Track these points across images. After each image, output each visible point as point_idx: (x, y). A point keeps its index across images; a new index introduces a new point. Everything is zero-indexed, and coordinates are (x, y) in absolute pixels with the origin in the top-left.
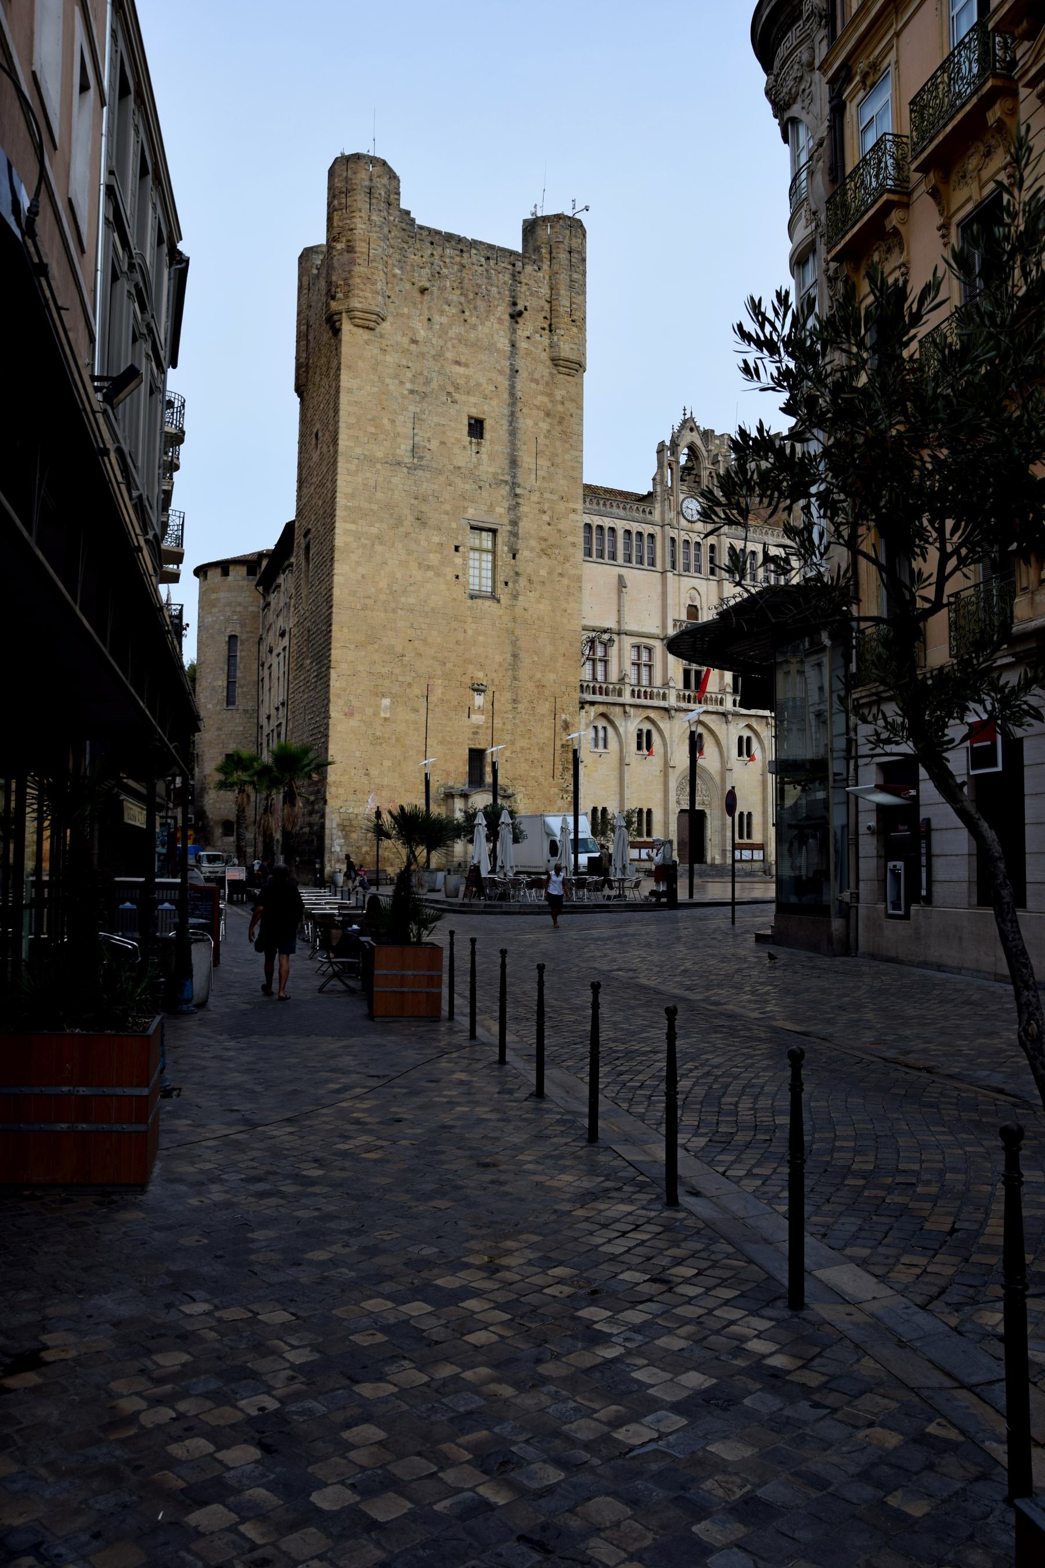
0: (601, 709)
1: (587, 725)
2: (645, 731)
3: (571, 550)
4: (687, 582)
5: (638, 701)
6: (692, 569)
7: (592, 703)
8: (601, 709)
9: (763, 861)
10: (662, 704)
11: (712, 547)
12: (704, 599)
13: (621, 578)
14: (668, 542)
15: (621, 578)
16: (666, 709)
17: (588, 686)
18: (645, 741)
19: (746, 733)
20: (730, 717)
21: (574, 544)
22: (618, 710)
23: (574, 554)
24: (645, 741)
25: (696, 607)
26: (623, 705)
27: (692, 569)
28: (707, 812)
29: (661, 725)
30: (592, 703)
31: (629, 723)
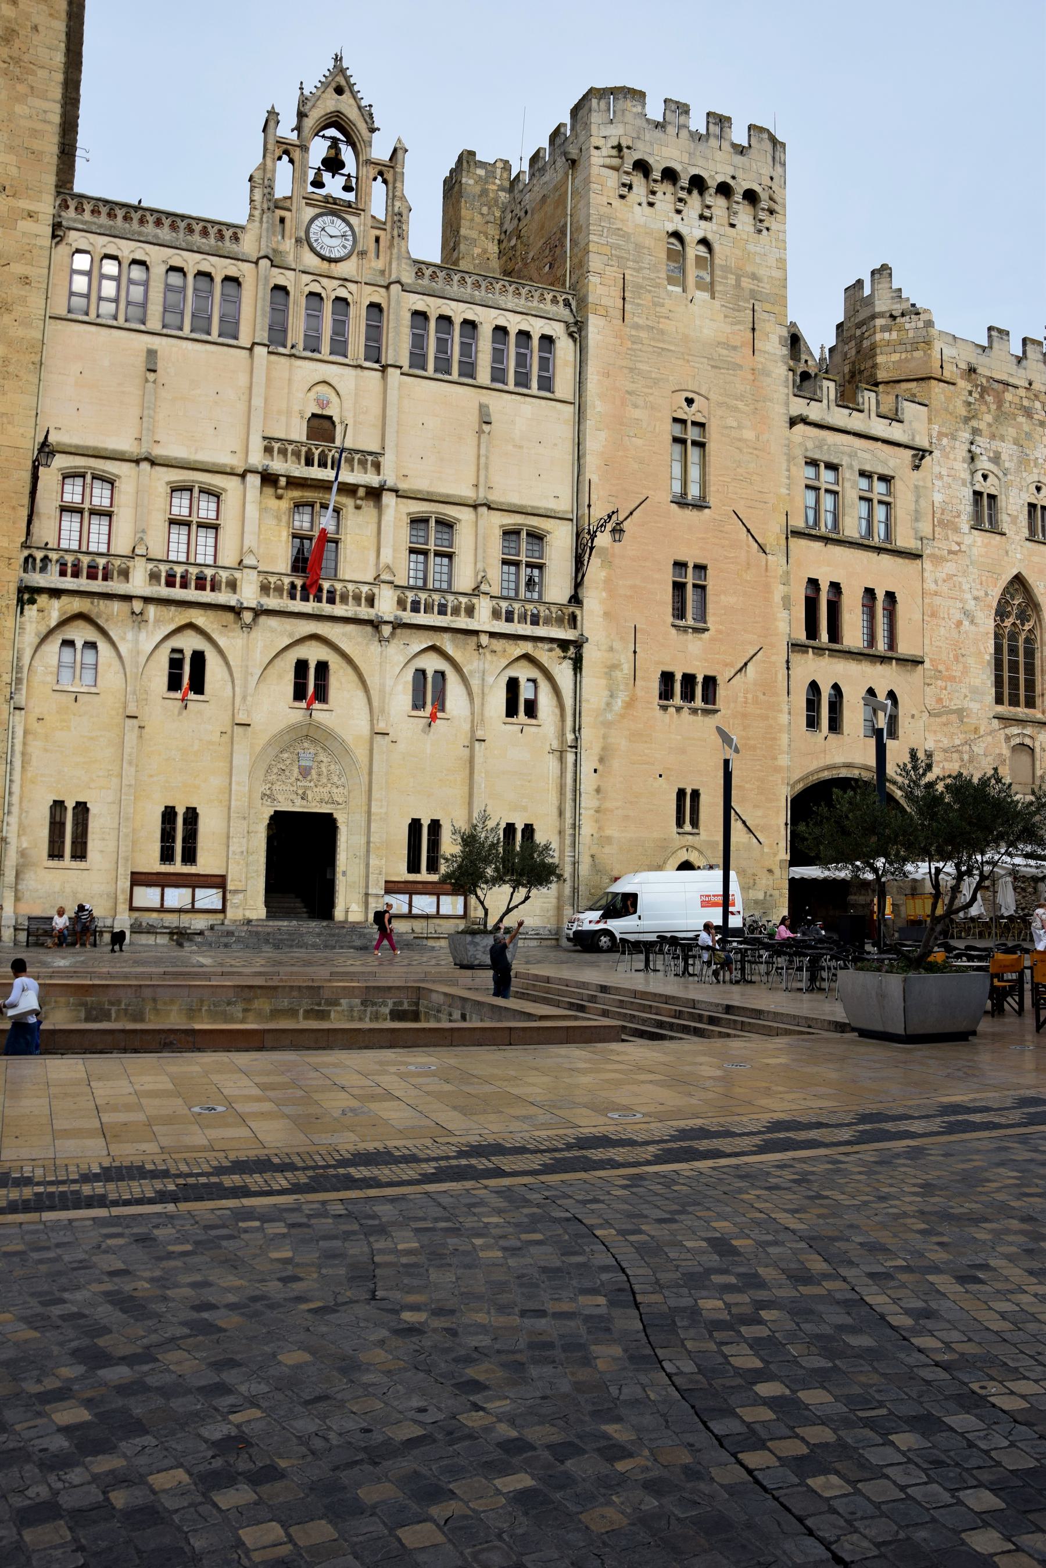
0: (77, 605)
1: (43, 640)
2: (188, 655)
3: (16, 290)
4: (309, 371)
5: (164, 592)
6: (326, 347)
7: (56, 593)
8: (77, 605)
9: (465, 916)
10: (223, 597)
11: (375, 307)
12: (348, 404)
13: (152, 354)
14: (265, 294)
15: (152, 354)
16: (230, 609)
17: (46, 559)
18: (188, 675)
19: (432, 664)
20: (387, 630)
21: (25, 280)
22: (116, 606)
23: (23, 300)
24: (188, 675)
25: (330, 418)
26: (127, 598)
27: (326, 347)
28: (340, 818)
29: (222, 642)
30: (56, 593)
31: (143, 636)
